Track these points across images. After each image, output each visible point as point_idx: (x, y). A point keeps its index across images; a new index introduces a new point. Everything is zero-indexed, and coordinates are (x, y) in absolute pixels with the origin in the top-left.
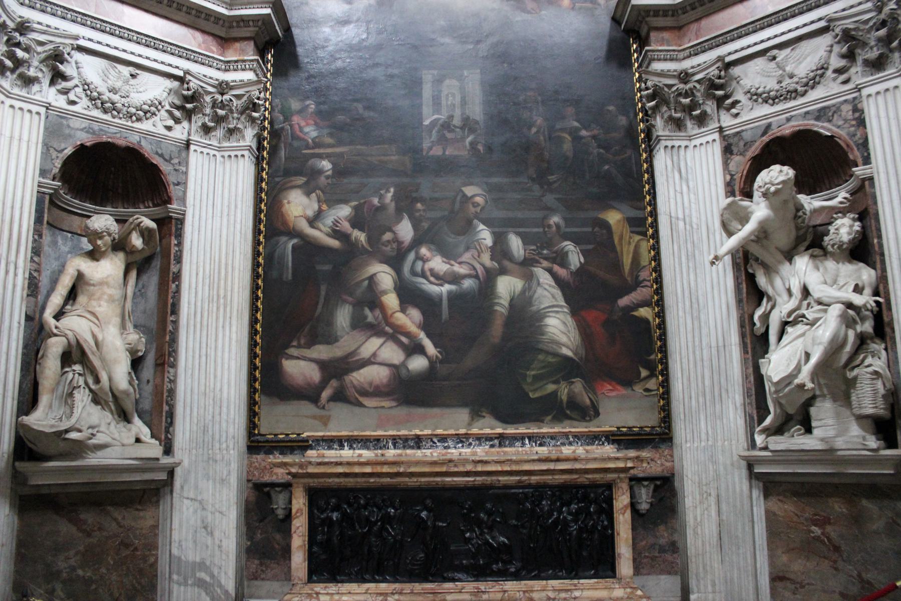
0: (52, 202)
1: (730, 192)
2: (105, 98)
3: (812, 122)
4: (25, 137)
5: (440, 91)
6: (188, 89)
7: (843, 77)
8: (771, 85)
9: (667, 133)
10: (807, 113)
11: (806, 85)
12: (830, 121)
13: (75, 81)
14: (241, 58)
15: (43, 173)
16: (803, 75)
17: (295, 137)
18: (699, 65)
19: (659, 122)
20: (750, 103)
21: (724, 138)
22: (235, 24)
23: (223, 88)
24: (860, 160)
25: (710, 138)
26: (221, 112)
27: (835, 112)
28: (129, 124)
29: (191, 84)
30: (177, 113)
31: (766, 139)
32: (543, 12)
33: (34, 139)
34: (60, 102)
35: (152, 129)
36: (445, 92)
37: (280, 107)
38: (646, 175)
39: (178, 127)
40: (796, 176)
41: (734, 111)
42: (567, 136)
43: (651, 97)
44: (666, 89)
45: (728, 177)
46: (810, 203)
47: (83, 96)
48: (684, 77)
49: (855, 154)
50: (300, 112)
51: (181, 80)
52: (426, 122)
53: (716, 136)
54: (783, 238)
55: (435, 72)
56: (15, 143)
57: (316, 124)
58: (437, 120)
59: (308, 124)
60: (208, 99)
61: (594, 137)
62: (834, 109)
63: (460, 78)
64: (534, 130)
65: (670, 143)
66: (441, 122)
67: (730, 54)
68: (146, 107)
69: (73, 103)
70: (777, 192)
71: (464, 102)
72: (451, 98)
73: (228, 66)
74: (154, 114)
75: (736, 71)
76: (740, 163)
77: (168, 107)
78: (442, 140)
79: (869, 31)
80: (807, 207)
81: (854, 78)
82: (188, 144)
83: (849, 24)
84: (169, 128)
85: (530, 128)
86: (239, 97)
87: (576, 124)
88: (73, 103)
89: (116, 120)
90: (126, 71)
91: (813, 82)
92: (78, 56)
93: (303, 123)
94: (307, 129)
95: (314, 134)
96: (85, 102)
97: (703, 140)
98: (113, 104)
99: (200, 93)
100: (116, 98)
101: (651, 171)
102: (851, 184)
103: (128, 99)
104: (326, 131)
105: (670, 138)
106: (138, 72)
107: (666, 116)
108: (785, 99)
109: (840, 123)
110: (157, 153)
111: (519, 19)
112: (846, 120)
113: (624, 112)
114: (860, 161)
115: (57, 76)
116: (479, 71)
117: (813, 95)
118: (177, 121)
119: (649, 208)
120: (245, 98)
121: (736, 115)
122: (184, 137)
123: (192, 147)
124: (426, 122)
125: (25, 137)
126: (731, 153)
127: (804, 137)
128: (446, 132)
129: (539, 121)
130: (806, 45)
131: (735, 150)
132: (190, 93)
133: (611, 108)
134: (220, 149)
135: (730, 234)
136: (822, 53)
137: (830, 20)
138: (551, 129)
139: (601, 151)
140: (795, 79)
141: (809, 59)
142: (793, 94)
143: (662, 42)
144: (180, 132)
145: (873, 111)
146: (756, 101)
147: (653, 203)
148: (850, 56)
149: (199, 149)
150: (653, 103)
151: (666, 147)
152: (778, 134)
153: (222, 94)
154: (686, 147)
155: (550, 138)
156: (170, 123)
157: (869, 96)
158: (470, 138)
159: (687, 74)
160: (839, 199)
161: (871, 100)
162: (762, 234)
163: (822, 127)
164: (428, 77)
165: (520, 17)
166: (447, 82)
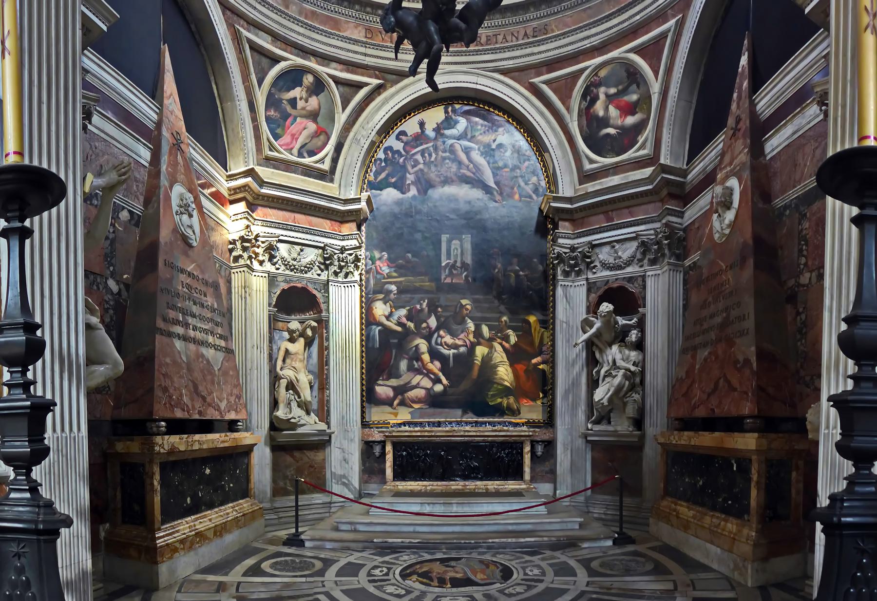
0: (274, 319)
1: (588, 312)
2: (290, 264)
3: (626, 283)
4: (262, 290)
5: (450, 247)
6: (327, 254)
7: (641, 264)
8: (611, 260)
9: (562, 278)
10: (624, 278)
11: (625, 264)
12: (633, 284)
13: (278, 258)
14: (350, 233)
15: (270, 305)
16: (625, 259)
17: (378, 272)
18: (581, 243)
19: (559, 272)
20: (601, 268)
21: (588, 284)
22: (346, 214)
23: (343, 250)
24: (642, 305)
25: (582, 283)
26: (343, 264)
27: (635, 280)
28: (302, 275)
29: (328, 251)
30: (322, 267)
31: (606, 287)
32: (504, 202)
33: (265, 290)
34: (272, 269)
35: (312, 276)
36: (453, 247)
37: (369, 256)
38: (551, 298)
39: (323, 274)
40: (614, 309)
41: (594, 270)
42: (513, 274)
43: (557, 258)
44: (564, 255)
45: (588, 304)
46: (621, 321)
47: (281, 265)
48: (573, 249)
49: (640, 302)
50: (380, 259)
51: (323, 249)
52: (443, 264)
53: (585, 282)
54: (607, 337)
55: (448, 236)
56: (258, 292)
57: (388, 265)
58: (449, 263)
59: (384, 266)
60: (336, 257)
61: (526, 275)
62: (635, 278)
63: (461, 240)
64: (496, 270)
65: (563, 283)
66: (450, 264)
67: (595, 240)
68: (308, 266)
69: (278, 269)
70: (605, 316)
71: (462, 254)
72: (455, 251)
73: (344, 238)
74: (312, 269)
75: (597, 250)
76: (594, 296)
77: (317, 264)
78: (451, 274)
79: (652, 244)
80: (620, 323)
81: (645, 265)
82: (328, 281)
83: (644, 238)
84: (319, 275)
85: (494, 270)
86: (351, 255)
87: (517, 268)
88: (278, 269)
89: (297, 274)
90: (298, 248)
91: (628, 263)
92: (279, 245)
93: (381, 265)
94: (383, 268)
95: (387, 271)
96: (283, 267)
97: (579, 283)
98: (294, 266)
99: (332, 255)
100: (295, 263)
101: (554, 296)
102: (639, 315)
103: (300, 263)
104: (393, 269)
105: (563, 280)
106: (303, 247)
107: (562, 269)
108: (616, 269)
109: (637, 286)
110: (314, 288)
111: (491, 206)
112: (639, 285)
113: (542, 264)
114: (642, 305)
115: (271, 258)
116: (470, 236)
117: (629, 269)
118: (322, 271)
119: (551, 315)
120: (354, 255)
121: (595, 273)
122: (326, 278)
123: (330, 283)
124: (443, 264)
125: (262, 290)
126: (591, 292)
127: (622, 289)
128: (453, 270)
129: (499, 265)
130: (628, 245)
131: (593, 291)
132: (328, 255)
133: (535, 260)
134: (343, 283)
135: (585, 332)
136: (634, 249)
137: (638, 235)
138: (505, 270)
139: (529, 283)
140: (621, 260)
141: (628, 251)
142: (620, 268)
143: (564, 228)
144: (324, 276)
145: (649, 283)
146: (604, 267)
147: (554, 312)
148: (644, 254)
149: (333, 284)
150: (557, 262)
151: (561, 285)
152: (611, 286)
153: (342, 253)
154: (571, 286)
155: (504, 275)
156: (319, 272)
157: (649, 276)
158: (465, 273)
159: (574, 247)
160: (633, 321)
161: (650, 278)
162: (598, 334)
163: (630, 286)
164: (444, 238)
165: (492, 204)
166: (454, 242)
